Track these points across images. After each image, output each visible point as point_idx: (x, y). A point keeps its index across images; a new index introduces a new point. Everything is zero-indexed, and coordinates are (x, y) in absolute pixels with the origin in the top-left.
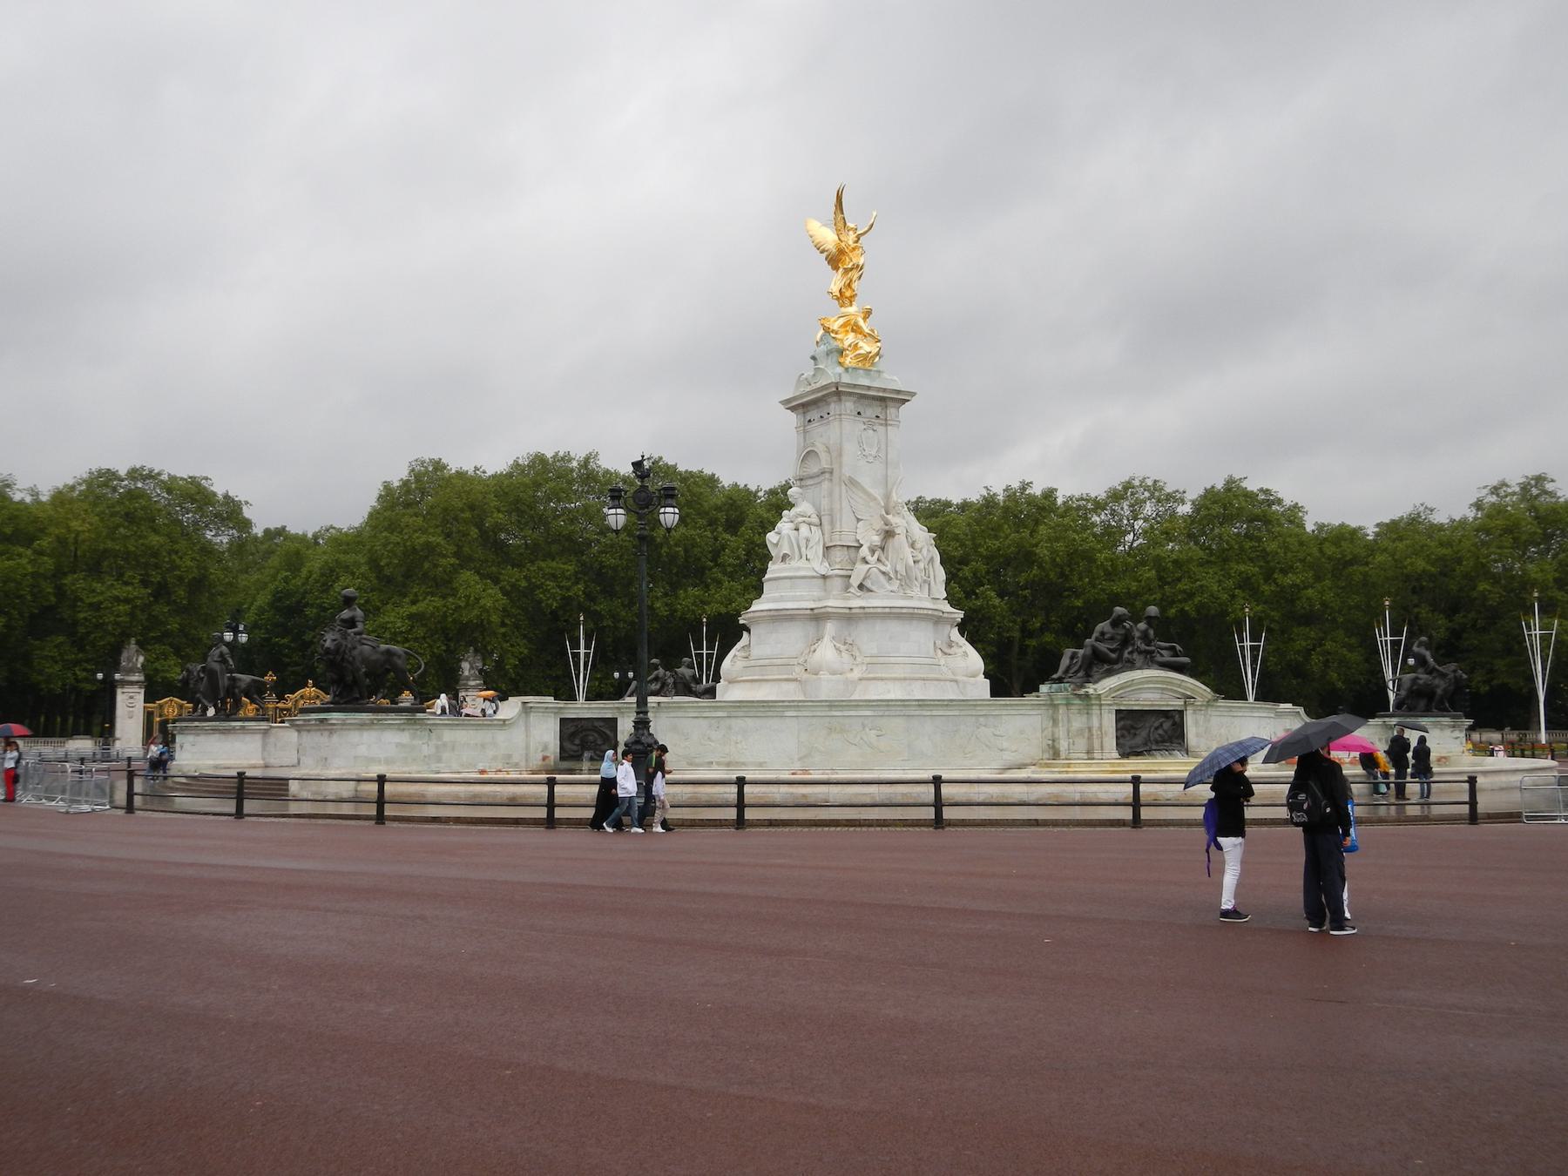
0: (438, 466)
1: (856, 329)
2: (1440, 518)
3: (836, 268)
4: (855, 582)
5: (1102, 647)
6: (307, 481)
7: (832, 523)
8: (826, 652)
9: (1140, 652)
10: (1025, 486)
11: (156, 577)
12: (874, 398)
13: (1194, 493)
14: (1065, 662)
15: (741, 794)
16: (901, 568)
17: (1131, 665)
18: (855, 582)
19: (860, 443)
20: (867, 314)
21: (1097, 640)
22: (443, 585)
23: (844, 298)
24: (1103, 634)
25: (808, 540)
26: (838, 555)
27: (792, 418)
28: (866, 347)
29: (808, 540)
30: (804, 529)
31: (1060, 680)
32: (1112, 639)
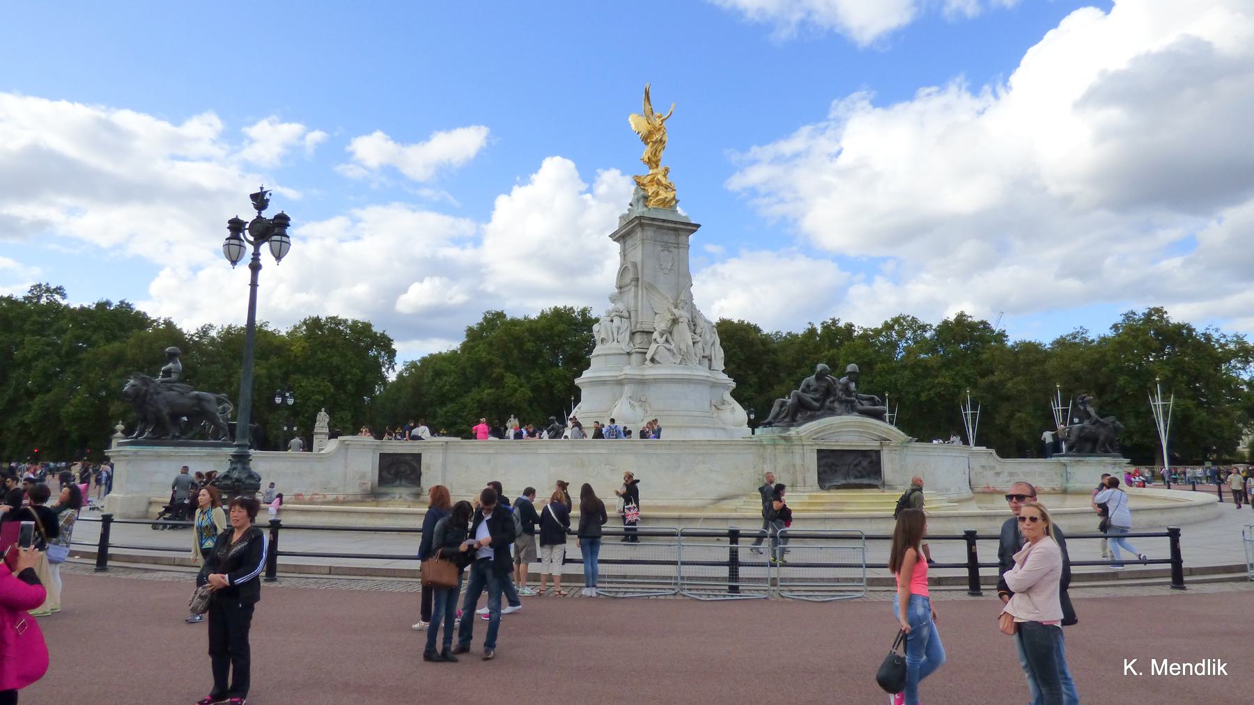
0: (500, 315)
1: (659, 183)
2: (1093, 335)
4: (648, 356)
5: (808, 397)
7: (637, 316)
9: (841, 402)
10: (834, 322)
11: (337, 378)
14: (775, 409)
16: (683, 347)
17: (832, 412)
18: (648, 356)
20: (667, 170)
21: (803, 391)
22: (498, 382)
24: (808, 386)
25: (619, 328)
26: (638, 338)
27: (616, 247)
28: (663, 194)
29: (619, 328)
31: (770, 424)
32: (816, 390)
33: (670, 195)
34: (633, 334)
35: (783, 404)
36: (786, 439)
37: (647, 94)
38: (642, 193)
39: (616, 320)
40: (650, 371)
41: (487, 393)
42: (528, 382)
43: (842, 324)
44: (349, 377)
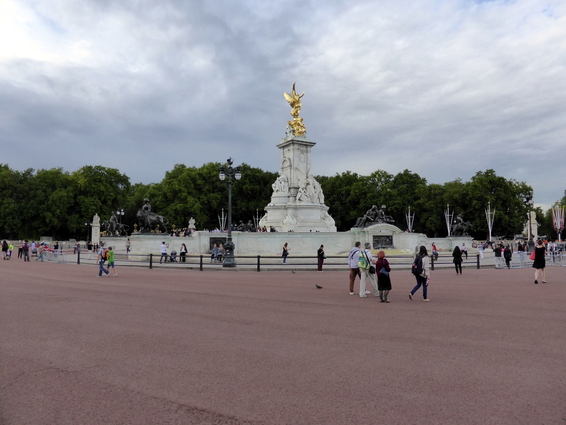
0: (183, 166)
1: (299, 125)
2: (464, 182)
3: (293, 107)
4: (298, 198)
6: (146, 170)
8: (289, 219)
12: (304, 145)
13: (395, 174)
15: (201, 260)
16: (311, 194)
19: (299, 157)
20: (302, 120)
22: (184, 201)
23: (295, 115)
26: (292, 190)
28: (300, 130)
30: (283, 182)
31: (357, 227)
33: (304, 130)
34: (290, 188)
35: (361, 220)
36: (364, 232)
37: (294, 86)
38: (292, 129)
39: (283, 182)
40: (298, 203)
41: (179, 206)
42: (199, 201)
43: (351, 174)
44: (108, 197)
